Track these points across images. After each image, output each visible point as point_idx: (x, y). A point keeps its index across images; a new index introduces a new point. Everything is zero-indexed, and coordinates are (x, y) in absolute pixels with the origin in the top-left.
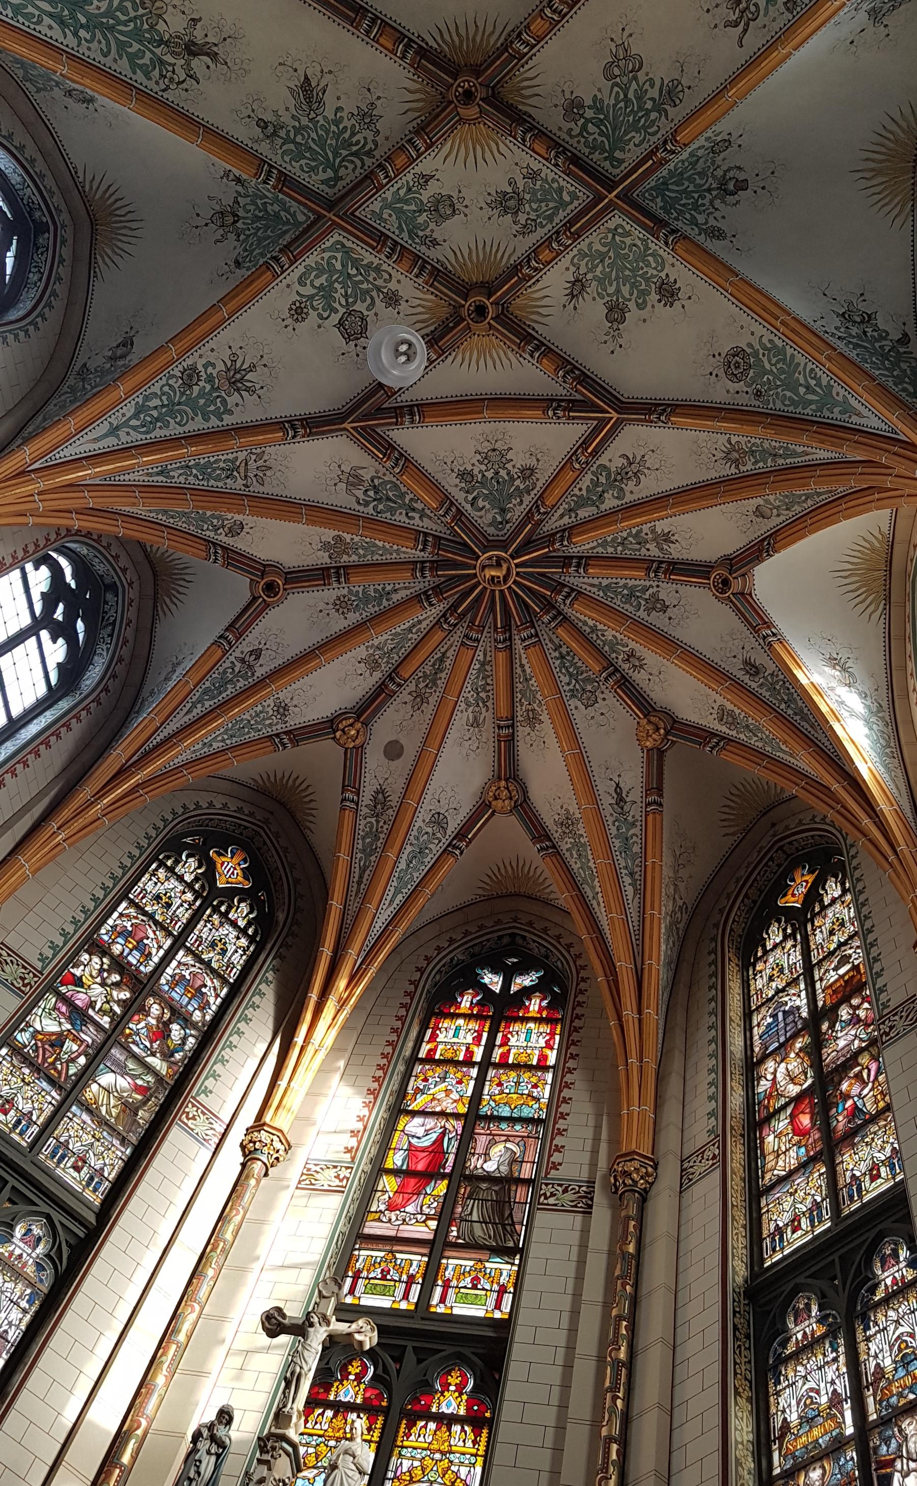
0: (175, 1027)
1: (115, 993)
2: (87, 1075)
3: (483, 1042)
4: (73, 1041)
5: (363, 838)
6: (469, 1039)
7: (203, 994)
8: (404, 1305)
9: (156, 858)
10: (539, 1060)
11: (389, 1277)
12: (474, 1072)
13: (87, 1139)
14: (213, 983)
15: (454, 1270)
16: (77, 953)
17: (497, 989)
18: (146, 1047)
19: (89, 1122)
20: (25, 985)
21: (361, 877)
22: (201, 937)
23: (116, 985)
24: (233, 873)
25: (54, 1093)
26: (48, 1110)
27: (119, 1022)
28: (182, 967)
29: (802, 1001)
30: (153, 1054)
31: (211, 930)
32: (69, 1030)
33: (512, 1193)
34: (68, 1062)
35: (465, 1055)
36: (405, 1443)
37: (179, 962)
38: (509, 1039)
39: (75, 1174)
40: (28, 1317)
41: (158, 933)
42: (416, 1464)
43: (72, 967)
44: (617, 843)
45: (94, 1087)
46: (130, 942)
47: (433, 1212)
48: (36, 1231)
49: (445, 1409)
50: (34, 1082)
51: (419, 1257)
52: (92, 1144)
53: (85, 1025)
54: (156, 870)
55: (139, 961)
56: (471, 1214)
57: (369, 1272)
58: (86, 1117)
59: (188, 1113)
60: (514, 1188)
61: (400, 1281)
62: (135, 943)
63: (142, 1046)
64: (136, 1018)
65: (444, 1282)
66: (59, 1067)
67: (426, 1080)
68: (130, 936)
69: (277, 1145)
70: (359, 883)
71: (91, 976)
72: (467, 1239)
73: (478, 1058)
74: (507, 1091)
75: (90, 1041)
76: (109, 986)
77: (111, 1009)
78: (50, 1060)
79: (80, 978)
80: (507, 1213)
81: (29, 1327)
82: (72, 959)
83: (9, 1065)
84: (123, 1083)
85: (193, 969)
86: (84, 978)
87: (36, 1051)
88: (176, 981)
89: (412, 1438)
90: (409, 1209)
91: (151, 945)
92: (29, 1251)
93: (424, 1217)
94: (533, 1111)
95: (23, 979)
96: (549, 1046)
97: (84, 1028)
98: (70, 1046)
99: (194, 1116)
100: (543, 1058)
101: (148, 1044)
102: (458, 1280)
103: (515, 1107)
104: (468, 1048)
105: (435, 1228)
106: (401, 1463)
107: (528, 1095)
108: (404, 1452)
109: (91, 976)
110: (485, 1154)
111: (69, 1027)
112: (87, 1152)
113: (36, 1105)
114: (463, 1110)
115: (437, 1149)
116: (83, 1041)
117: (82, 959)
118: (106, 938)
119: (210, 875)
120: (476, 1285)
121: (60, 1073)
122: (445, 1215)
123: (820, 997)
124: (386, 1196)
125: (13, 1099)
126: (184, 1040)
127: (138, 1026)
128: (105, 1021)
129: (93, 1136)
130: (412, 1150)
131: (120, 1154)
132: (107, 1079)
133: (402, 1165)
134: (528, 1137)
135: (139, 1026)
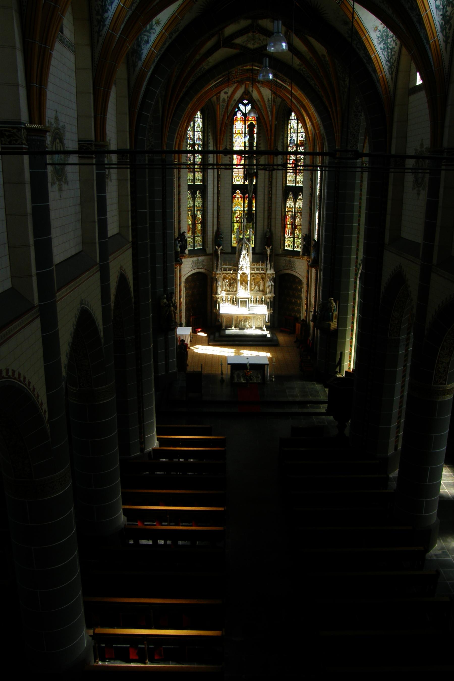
5: (222, 106)
21: (222, 112)
29: (295, 139)
44: (268, 107)
58: (197, 173)
67: (236, 138)
70: (222, 113)
73: (244, 132)
123: (298, 141)
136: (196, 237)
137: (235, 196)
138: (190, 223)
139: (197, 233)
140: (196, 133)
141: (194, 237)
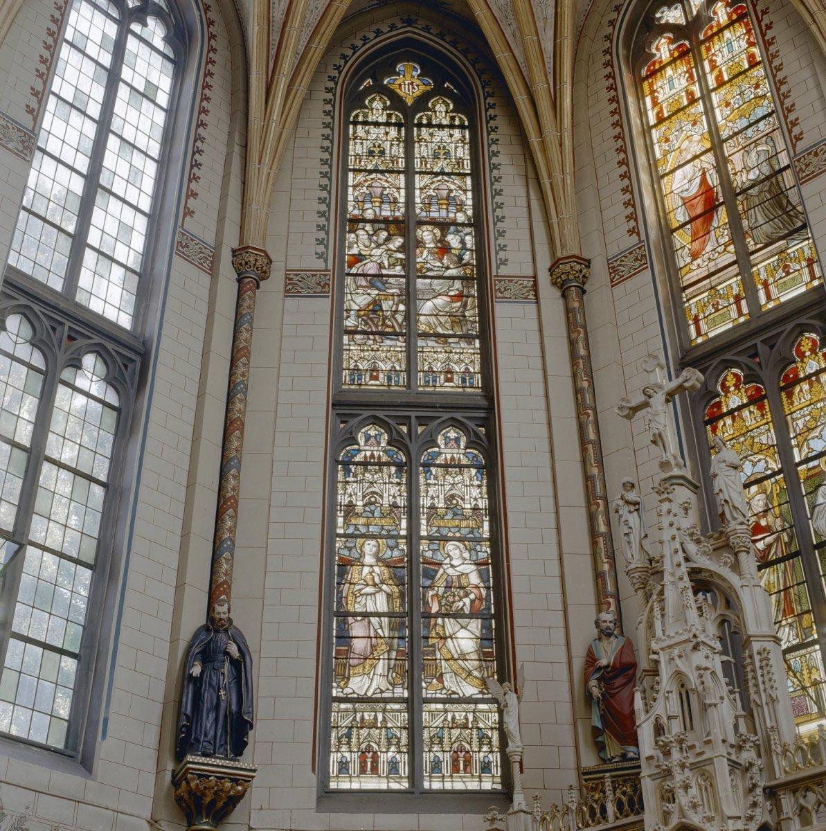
0: (450, 238)
1: (391, 246)
2: (410, 316)
3: (696, 79)
4: (386, 299)
6: (684, 82)
7: (454, 198)
8: (742, 320)
9: (347, 123)
10: (749, 62)
11: (720, 307)
12: (700, 107)
13: (443, 356)
14: (455, 184)
15: (766, 271)
16: (343, 239)
17: (682, 21)
18: (439, 267)
19: (436, 345)
20: (324, 287)
22: (423, 157)
23: (388, 239)
24: (413, 88)
25: (399, 344)
26: (402, 356)
27: (407, 264)
28: (425, 191)
30: (448, 268)
31: (426, 146)
32: (378, 295)
33: (782, 185)
34: (393, 316)
35: (688, 99)
36: (793, 410)
37: (421, 189)
38: (715, 61)
39: (452, 384)
40: (485, 489)
41: (389, 180)
42: (808, 418)
43: (349, 251)
45: (422, 318)
46: (375, 202)
47: (727, 239)
48: (452, 435)
49: (810, 371)
50: (380, 346)
51: (735, 279)
52: (448, 357)
53: (387, 283)
54: (355, 132)
55: (391, 211)
56: (756, 221)
57: (704, 313)
58: (431, 343)
59: (499, 289)
60: (780, 178)
61: (730, 305)
62: (379, 200)
63: (436, 269)
64: (418, 251)
65: (763, 284)
66: (389, 323)
68: (372, 197)
69: (578, 267)
71: (366, 247)
72: (763, 241)
74: (737, 106)
75: (398, 291)
76: (383, 244)
77: (397, 259)
78: (380, 323)
79: (360, 254)
80: (785, 202)
81: (488, 493)
82: (341, 244)
83: (356, 347)
84: (440, 301)
85: (433, 186)
86: (362, 252)
87: (366, 324)
88: (427, 205)
89: (796, 403)
90: (708, 248)
91: (391, 192)
92: (456, 451)
93: (723, 247)
94: (765, 108)
95: (319, 284)
96: (751, 44)
97: (387, 285)
98: (387, 305)
99: (505, 288)
100: (751, 57)
101: (439, 264)
102: (773, 276)
103: (750, 115)
104: (687, 92)
105: (733, 250)
106: (797, 424)
107: (755, 98)
108: (794, 416)
109: (366, 247)
110: (745, 168)
111: (376, 292)
112: (449, 364)
113: (393, 360)
114: (708, 145)
115: (706, 190)
116: (393, 295)
117: (351, 240)
118: (356, 212)
119: (396, 102)
120: (788, 271)
121: (393, 327)
122: (738, 234)
124: (686, 250)
125: (375, 366)
126: (463, 242)
127: (423, 256)
128: (398, 270)
129: (446, 352)
130: (686, 202)
131: (472, 351)
132: (427, 307)
133: (685, 219)
134: (774, 130)
135: (424, 257)
136: (436, 701)
137: (719, 405)
138: (371, 608)
139: (440, 678)
140: (419, 181)
141: (413, 704)
